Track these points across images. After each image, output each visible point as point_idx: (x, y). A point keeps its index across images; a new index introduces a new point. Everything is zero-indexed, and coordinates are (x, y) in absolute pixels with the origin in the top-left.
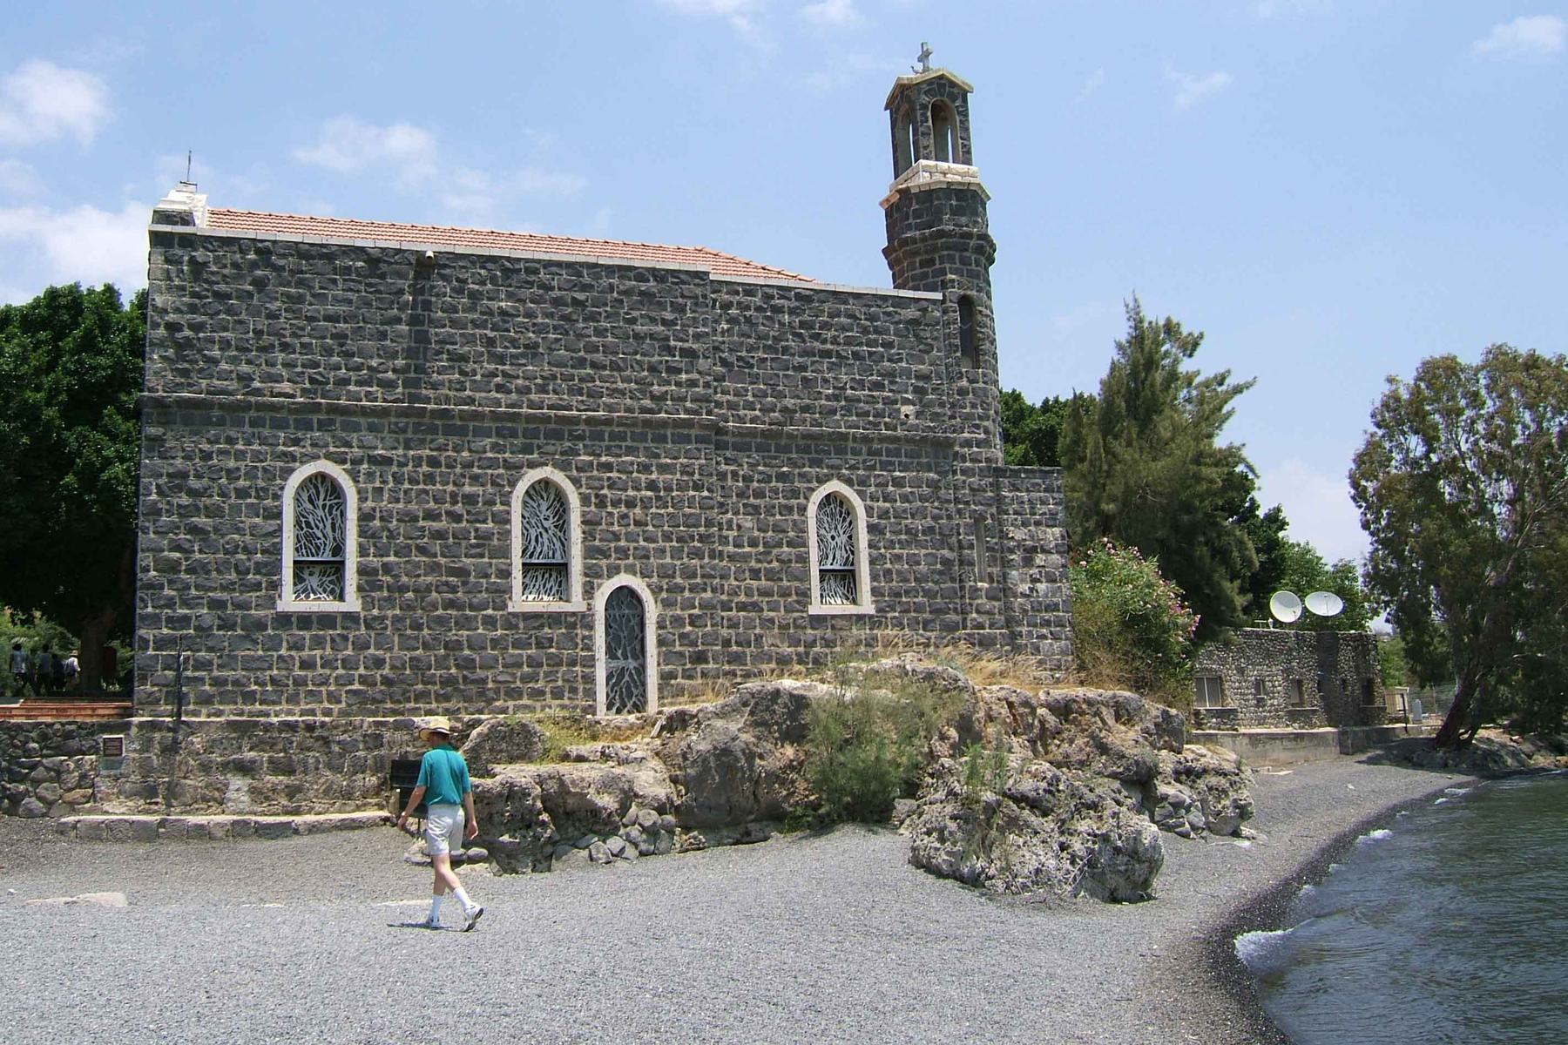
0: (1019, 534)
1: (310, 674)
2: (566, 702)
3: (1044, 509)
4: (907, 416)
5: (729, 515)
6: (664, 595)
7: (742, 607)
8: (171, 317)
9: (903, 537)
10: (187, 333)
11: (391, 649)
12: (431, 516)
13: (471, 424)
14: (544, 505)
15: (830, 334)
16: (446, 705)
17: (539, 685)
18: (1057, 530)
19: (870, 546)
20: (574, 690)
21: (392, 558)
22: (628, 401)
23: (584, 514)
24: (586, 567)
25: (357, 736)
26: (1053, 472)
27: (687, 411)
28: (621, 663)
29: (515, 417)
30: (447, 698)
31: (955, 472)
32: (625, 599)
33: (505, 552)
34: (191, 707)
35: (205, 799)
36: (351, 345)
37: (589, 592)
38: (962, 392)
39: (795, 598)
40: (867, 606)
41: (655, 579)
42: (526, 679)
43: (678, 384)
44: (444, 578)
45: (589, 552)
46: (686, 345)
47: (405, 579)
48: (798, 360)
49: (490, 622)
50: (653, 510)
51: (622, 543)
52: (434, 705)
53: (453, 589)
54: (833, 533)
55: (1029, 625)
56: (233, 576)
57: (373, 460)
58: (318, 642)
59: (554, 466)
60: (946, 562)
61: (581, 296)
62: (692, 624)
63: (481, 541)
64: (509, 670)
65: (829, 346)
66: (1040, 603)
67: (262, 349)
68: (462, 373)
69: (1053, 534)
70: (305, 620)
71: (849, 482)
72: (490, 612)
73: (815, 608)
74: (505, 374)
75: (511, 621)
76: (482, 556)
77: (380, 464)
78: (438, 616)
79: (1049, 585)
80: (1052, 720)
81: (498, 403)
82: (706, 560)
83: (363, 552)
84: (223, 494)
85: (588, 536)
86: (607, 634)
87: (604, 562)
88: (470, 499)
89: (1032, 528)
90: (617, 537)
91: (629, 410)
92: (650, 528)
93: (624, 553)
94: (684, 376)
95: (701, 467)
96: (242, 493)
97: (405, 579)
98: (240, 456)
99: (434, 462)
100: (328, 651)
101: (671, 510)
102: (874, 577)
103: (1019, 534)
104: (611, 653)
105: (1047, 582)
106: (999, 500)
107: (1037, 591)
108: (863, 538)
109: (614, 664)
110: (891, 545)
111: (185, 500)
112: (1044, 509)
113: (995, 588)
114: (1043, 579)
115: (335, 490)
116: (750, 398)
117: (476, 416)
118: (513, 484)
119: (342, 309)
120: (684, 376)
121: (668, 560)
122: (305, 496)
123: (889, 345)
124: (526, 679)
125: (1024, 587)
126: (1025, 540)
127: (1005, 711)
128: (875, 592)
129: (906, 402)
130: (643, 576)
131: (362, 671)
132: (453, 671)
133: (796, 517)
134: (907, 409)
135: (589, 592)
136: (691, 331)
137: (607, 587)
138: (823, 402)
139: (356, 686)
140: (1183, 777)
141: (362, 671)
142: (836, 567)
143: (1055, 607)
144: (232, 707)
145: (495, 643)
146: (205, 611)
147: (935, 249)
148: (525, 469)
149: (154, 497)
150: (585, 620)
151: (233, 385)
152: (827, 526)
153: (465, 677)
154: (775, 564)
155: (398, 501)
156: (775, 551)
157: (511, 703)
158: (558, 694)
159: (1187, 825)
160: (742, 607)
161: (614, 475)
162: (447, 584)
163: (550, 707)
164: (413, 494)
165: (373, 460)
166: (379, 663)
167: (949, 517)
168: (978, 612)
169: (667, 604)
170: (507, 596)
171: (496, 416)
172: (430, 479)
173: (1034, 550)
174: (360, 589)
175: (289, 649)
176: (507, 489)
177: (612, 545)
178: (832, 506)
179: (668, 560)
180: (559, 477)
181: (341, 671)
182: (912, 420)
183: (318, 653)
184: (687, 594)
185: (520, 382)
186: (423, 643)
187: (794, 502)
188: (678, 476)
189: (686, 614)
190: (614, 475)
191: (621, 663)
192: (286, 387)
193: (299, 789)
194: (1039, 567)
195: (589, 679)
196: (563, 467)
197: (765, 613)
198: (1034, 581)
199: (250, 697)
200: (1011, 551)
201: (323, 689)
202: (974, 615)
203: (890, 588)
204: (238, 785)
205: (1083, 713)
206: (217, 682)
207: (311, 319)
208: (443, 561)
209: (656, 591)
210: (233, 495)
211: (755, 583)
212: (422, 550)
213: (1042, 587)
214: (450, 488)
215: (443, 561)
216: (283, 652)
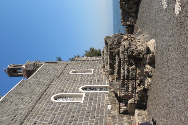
2: (105, 96)
9: (81, 67)
11: (88, 123)
12: (54, 114)
13: (35, 108)
17: (101, 99)
21: (63, 122)
25: (112, 120)
44: (72, 113)
45: (73, 92)
49: (84, 106)
52: (104, 115)
59: (51, 96)
63: (64, 107)
64: (97, 103)
68: (21, 109)
71: (70, 71)
72: (82, 106)
75: (85, 103)
77: (35, 123)
78: (81, 114)
85: (69, 92)
87: (75, 91)
99: (41, 114)
106: (78, 61)
129: (59, 67)
132: (96, 112)
147: (36, 65)
148: (50, 101)
157: (105, 103)
162: (73, 112)
164: (47, 118)
170: (79, 103)
176: (53, 103)
186: (87, 116)
189: (89, 82)
208: (67, 113)
212: (63, 116)
214: (49, 111)
215: (67, 113)
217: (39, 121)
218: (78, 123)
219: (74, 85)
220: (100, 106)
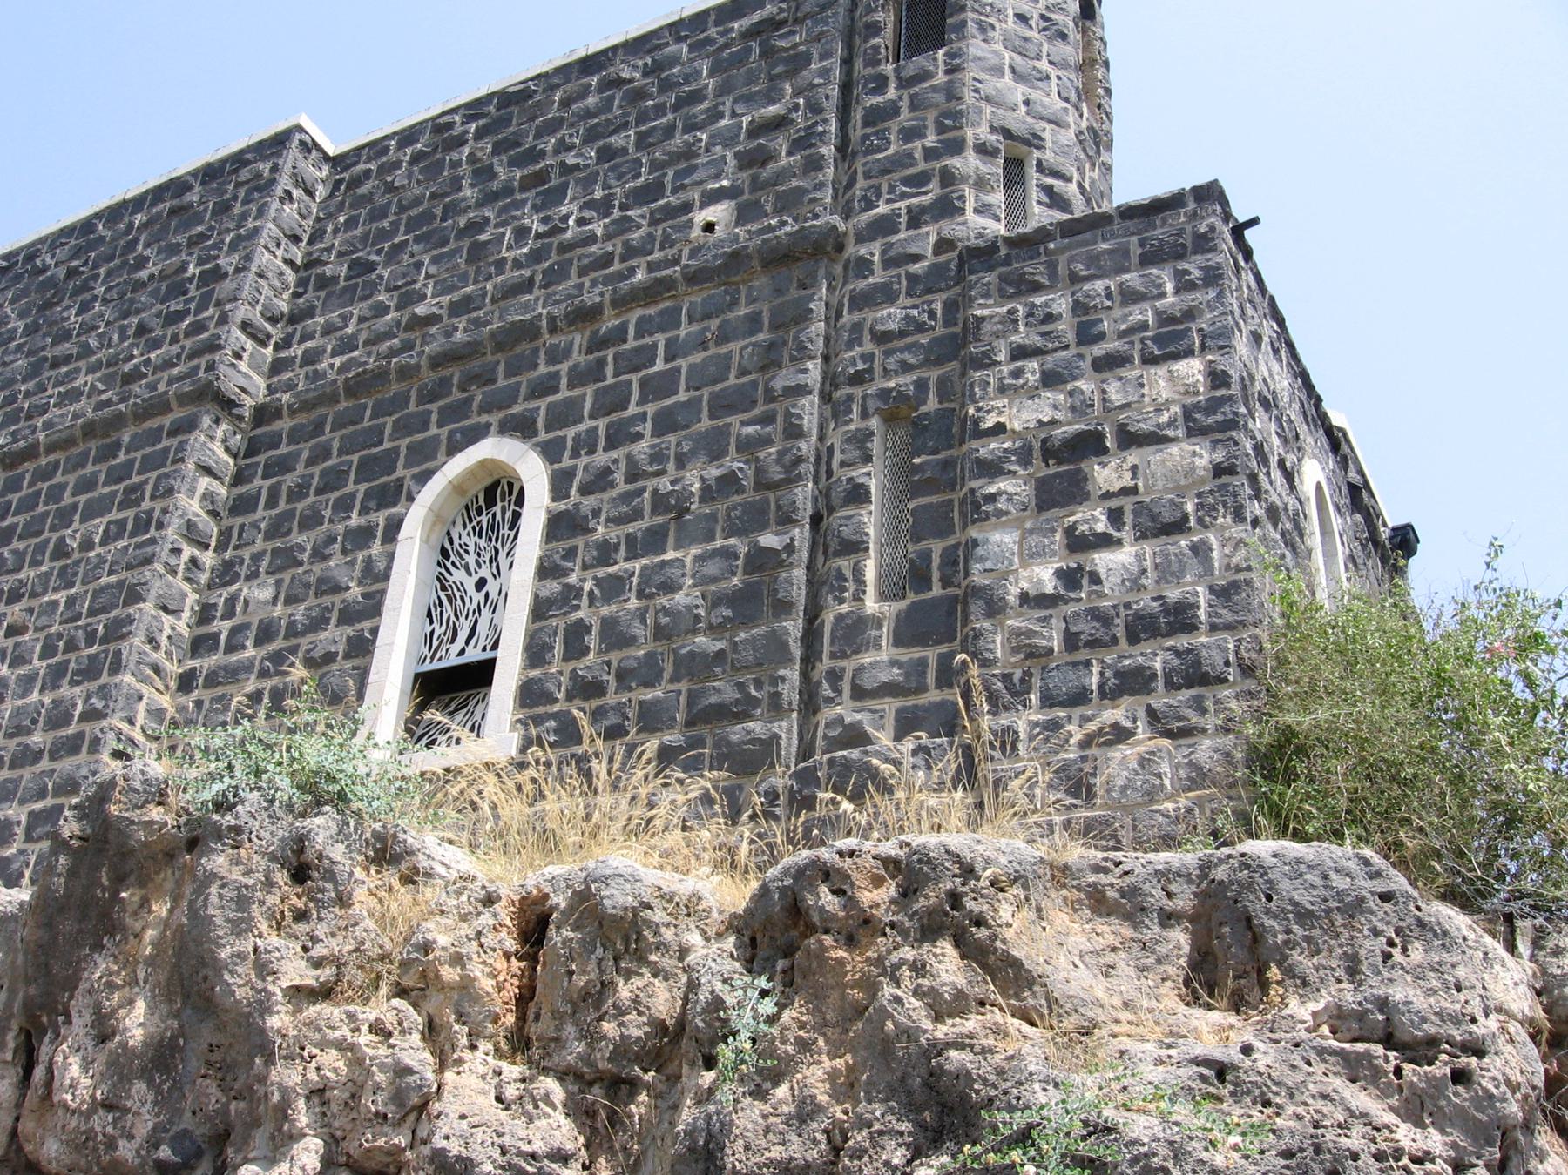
3: (1143, 313)
54: (485, 572)
55: (1048, 701)
66: (1101, 617)
79: (1147, 548)
89: (1085, 385)
105: (1142, 536)
107: (1095, 579)
110: (605, 553)
112: (1143, 313)
113: (935, 601)
114: (1127, 534)
126: (1053, 422)
134: (718, 213)
152: (471, 559)
178: (497, 509)
194: (1107, 495)
198: (1080, 543)
200: (992, 469)
203: (574, 675)
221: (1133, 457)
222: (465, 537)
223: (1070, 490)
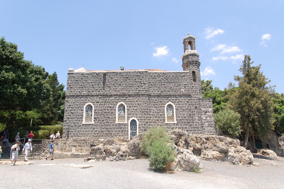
0: (203, 109)
1: (86, 133)
2: (124, 137)
4: (183, 91)
5: (152, 108)
6: (140, 120)
7: (154, 122)
8: (70, 84)
10: (72, 86)
11: (98, 129)
12: (104, 110)
14: (122, 108)
15: (169, 79)
16: (106, 137)
17: (120, 134)
18: (211, 109)
19: (176, 112)
20: (125, 135)
22: (135, 91)
23: (127, 109)
24: (128, 116)
26: (210, 99)
27: (144, 92)
28: (133, 131)
29: (117, 95)
30: (106, 136)
31: (191, 100)
32: (133, 122)
33: (115, 115)
34: (70, 137)
35: (69, 151)
36: (94, 86)
37: (128, 120)
38: (193, 87)
39: (163, 121)
40: (175, 122)
41: (138, 118)
42: (118, 133)
43: (143, 88)
45: (128, 114)
46: (144, 82)
47: (100, 119)
48: (163, 84)
49: (113, 125)
50: (138, 108)
51: (133, 113)
53: (107, 120)
56: (77, 119)
57: (97, 102)
58: (88, 128)
60: (190, 115)
61: (128, 77)
62: (144, 125)
65: (169, 81)
67: (82, 88)
68: (109, 89)
69: (210, 110)
70: (86, 124)
71: (173, 102)
72: (113, 123)
73: (166, 122)
74: (116, 89)
76: (112, 115)
80: (205, 140)
81: (115, 93)
82: (147, 115)
83: (95, 115)
84: (76, 108)
85: (128, 112)
86: (131, 126)
87: (130, 116)
88: (110, 107)
90: (132, 112)
91: (134, 93)
92: (138, 110)
93: (133, 114)
94: (143, 87)
95: (146, 101)
96: (79, 108)
97: (100, 119)
98: (78, 102)
99: (105, 102)
100: (89, 130)
101: (141, 107)
102: (177, 117)
103: (203, 109)
104: (131, 129)
108: (175, 111)
109: (132, 131)
111: (71, 109)
112: (209, 105)
115: (92, 107)
116: (156, 90)
117: (111, 95)
118: (116, 105)
119: (93, 81)
120: (143, 87)
121: (140, 115)
122: (87, 108)
123: (180, 80)
124: (118, 133)
125: (204, 118)
127: (195, 139)
128: (177, 120)
130: (136, 117)
131: (94, 132)
133: (163, 108)
135: (128, 120)
136: (145, 80)
137: (131, 119)
138: (168, 90)
139: (93, 134)
140: (236, 152)
141: (94, 132)
142: (170, 116)
143: (211, 122)
144: (76, 137)
145: (113, 128)
146: (73, 124)
149: (67, 109)
150: (127, 124)
151: (78, 93)
153: (109, 133)
154: (159, 115)
155: (100, 108)
156: (159, 113)
157: (115, 137)
158: (123, 136)
159: (235, 161)
160: (154, 122)
161: (132, 103)
163: (121, 138)
165: (97, 102)
166: (96, 131)
167: (190, 107)
168: (196, 123)
169: (140, 122)
171: (114, 95)
172: (105, 104)
173: (207, 112)
174: (94, 120)
175: (84, 129)
176: (116, 105)
177: (132, 113)
179: (140, 115)
180: (123, 103)
181: (91, 132)
182: (184, 92)
183: (88, 130)
184: (143, 120)
185: (118, 90)
187: (163, 105)
188: (142, 102)
190: (132, 103)
191: (133, 131)
192: (85, 93)
193: (82, 149)
195: (128, 134)
196: (124, 102)
197: (158, 123)
199: (78, 136)
201: (88, 135)
202: (195, 123)
204: (74, 148)
205: (211, 139)
206: (74, 134)
207: (88, 83)
208: (106, 116)
209: (138, 120)
210: (77, 108)
211: (156, 119)
212: (103, 115)
213: (208, 118)
216: (83, 130)
217: (99, 103)
218: (98, 124)
219: (138, 113)
220: (113, 134)
221: (209, 113)
222: (168, 108)
223: (205, 114)
